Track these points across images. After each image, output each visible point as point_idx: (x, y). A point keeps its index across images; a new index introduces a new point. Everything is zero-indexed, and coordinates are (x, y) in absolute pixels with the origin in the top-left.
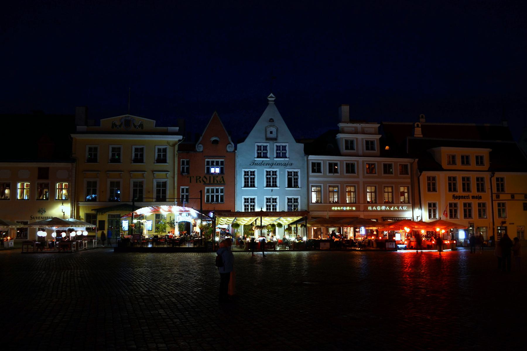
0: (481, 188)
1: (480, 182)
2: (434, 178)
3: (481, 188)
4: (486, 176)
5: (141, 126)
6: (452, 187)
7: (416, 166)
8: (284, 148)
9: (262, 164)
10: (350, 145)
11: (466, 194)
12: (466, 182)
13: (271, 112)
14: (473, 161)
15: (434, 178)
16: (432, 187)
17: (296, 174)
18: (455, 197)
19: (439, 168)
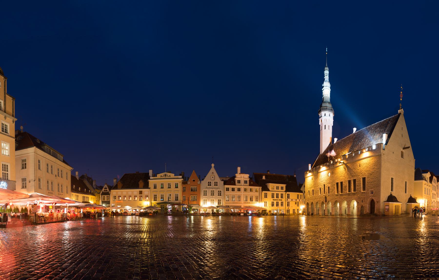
0: (282, 197)
1: (282, 195)
2: (267, 194)
3: (282, 197)
4: (284, 193)
5: (170, 176)
6: (273, 197)
7: (261, 189)
8: (217, 182)
9: (209, 188)
10: (239, 182)
11: (277, 199)
12: (277, 195)
13: (213, 170)
14: (280, 188)
15: (267, 194)
16: (266, 196)
17: (221, 191)
18: (273, 200)
19: (268, 190)
